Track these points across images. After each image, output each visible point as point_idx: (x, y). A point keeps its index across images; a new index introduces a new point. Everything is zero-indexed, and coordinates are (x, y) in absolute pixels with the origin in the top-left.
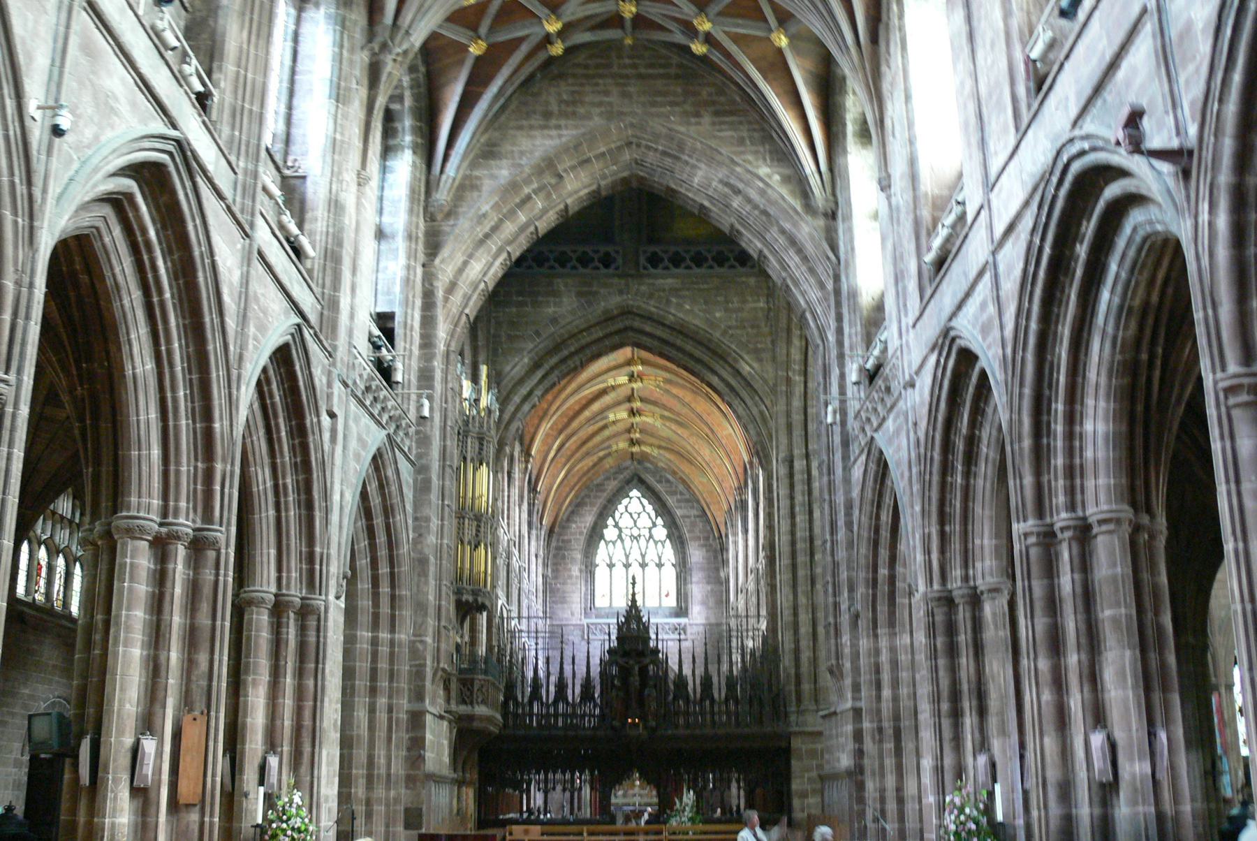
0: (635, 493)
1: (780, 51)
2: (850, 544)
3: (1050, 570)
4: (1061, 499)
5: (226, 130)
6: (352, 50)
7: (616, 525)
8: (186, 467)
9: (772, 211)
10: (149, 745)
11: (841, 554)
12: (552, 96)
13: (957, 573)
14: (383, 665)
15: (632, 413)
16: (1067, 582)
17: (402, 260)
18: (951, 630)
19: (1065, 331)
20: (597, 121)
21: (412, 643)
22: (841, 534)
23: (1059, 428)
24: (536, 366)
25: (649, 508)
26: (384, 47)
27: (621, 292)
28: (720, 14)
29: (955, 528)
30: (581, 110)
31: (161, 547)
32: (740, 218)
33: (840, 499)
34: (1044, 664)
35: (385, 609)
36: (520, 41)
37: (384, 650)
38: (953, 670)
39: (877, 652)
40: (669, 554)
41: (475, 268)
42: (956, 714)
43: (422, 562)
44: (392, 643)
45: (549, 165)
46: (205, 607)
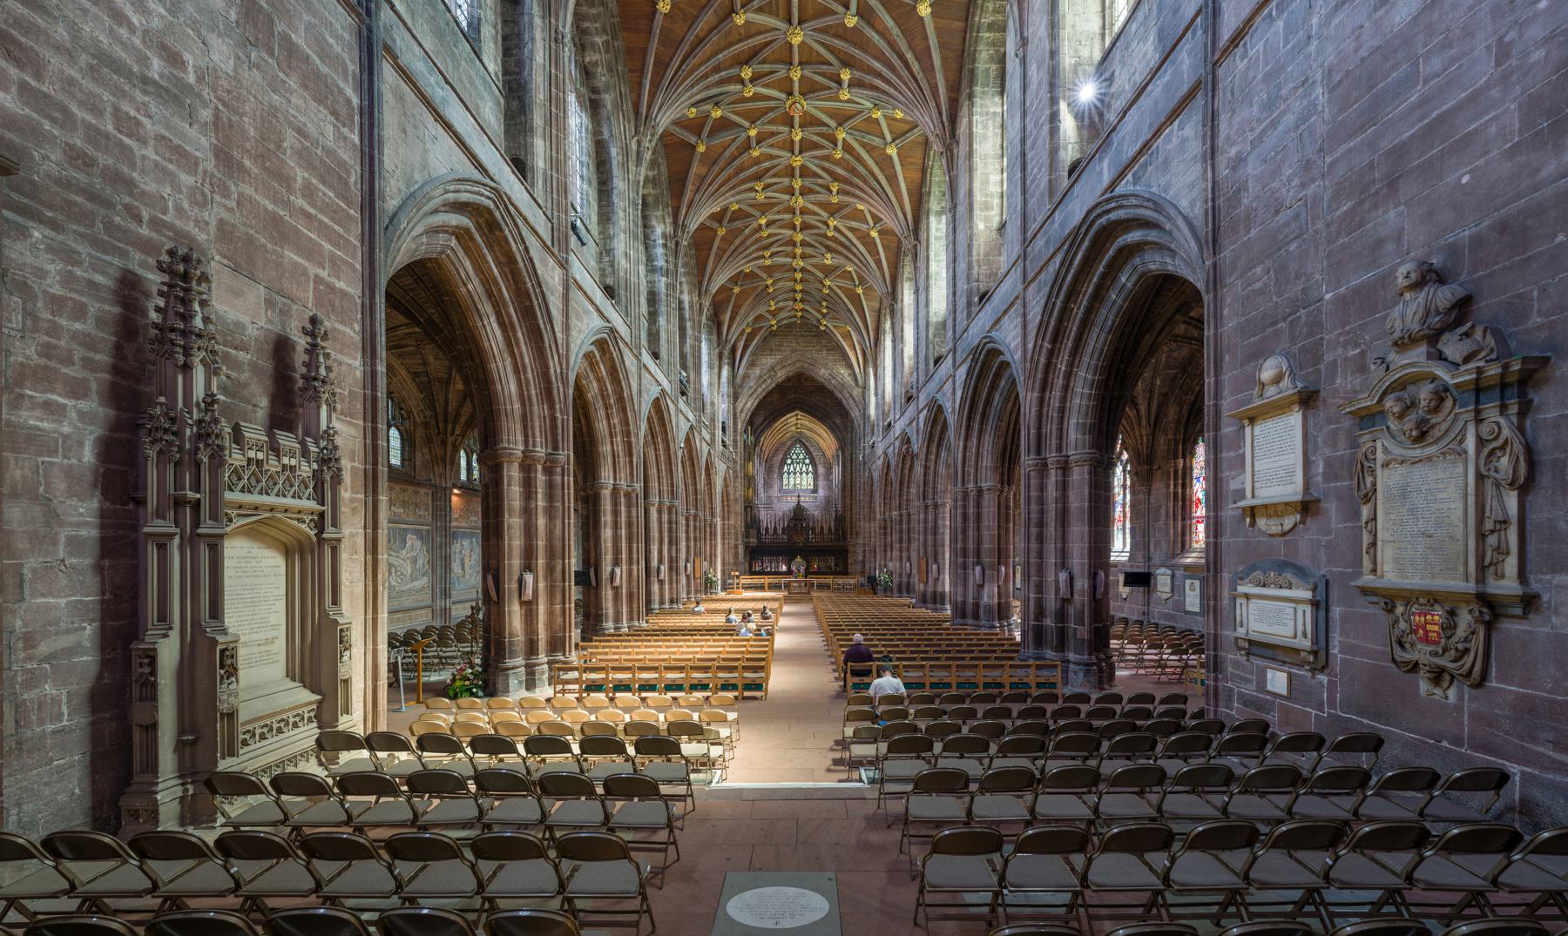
3: (901, 522)
12: (773, 343)
18: (885, 528)
45: (772, 369)
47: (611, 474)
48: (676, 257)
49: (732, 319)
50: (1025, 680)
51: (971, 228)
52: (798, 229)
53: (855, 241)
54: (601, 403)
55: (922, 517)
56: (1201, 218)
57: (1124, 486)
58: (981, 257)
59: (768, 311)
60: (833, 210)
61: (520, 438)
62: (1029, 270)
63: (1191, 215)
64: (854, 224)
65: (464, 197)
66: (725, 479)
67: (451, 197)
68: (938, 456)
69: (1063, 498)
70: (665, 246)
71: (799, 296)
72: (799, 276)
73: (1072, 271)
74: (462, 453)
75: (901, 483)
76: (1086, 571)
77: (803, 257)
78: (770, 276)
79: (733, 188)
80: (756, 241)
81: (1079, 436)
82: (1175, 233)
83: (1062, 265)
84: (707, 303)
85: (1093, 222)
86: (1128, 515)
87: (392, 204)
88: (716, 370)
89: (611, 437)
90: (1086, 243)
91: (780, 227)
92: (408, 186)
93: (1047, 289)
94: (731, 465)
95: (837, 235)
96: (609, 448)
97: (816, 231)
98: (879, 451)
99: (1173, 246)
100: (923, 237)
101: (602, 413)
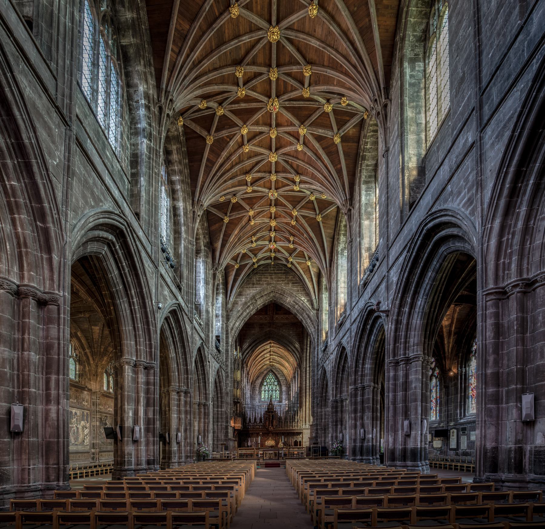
6: (209, 270)
9: (304, 309)
15: (270, 355)
26: (216, 269)
27: (269, 327)
40: (278, 388)
45: (254, 297)
78: (252, 208)
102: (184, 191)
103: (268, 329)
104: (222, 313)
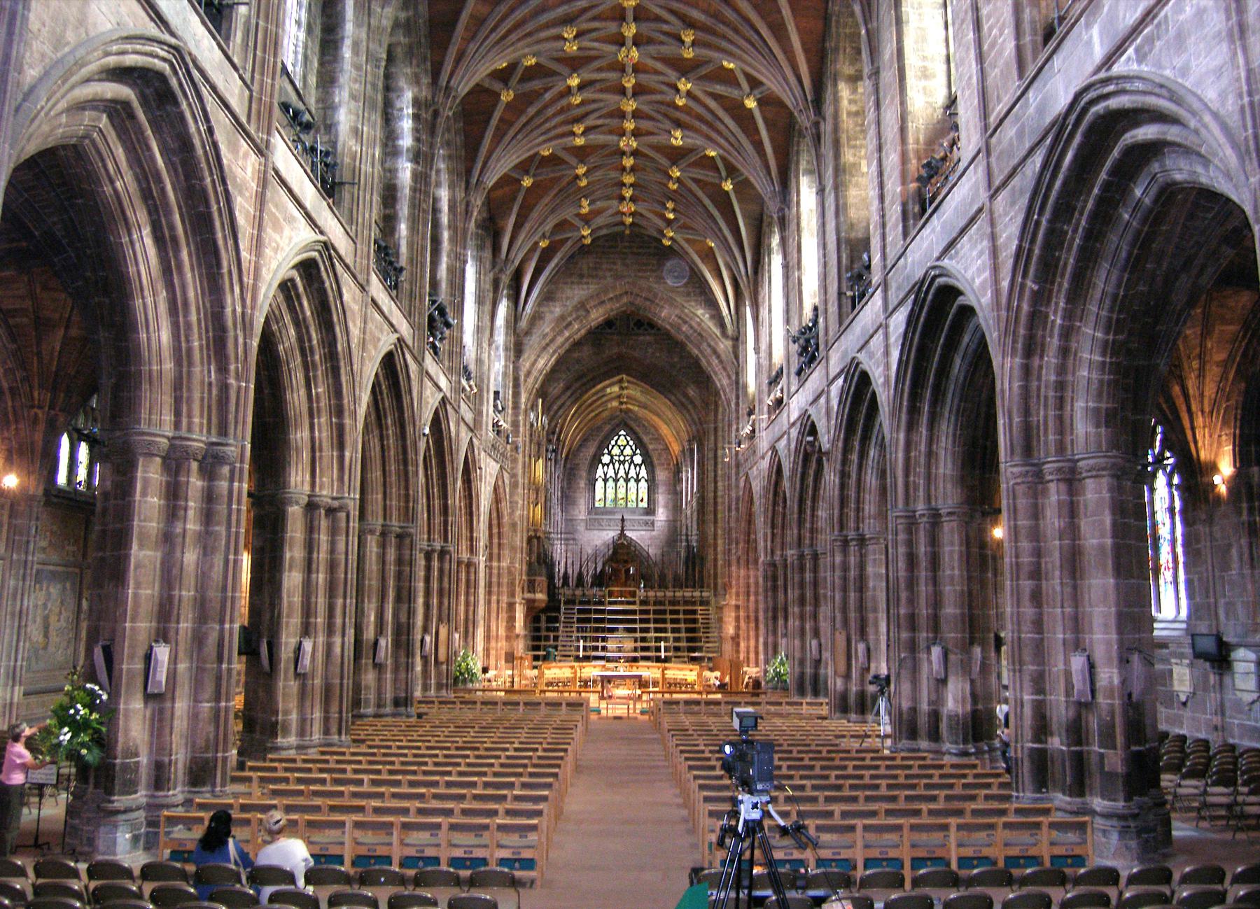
0: (622, 432)
1: (711, 248)
2: (737, 520)
3: (802, 569)
4: (807, 542)
5: (447, 363)
7: (609, 453)
8: (437, 520)
10: (428, 638)
11: (733, 525)
12: (585, 264)
13: (779, 553)
14: (495, 579)
15: (622, 388)
16: (808, 576)
17: (503, 363)
18: (775, 579)
19: (812, 472)
20: (609, 280)
21: (509, 568)
22: (734, 513)
23: (808, 512)
24: (567, 388)
25: (631, 443)
26: (501, 271)
28: (680, 227)
29: (778, 531)
30: (601, 273)
31: (428, 556)
32: (687, 337)
33: (734, 495)
34: (796, 610)
35: (495, 551)
36: (567, 239)
37: (495, 571)
38: (775, 598)
39: (749, 577)
40: (643, 473)
41: (541, 362)
42: (775, 618)
43: (514, 525)
44: (499, 568)
45: (582, 306)
46: (446, 579)
47: (308, 477)
48: (433, 133)
49: (518, 226)
50: (1032, 852)
51: (903, 103)
52: (629, 92)
53: (721, 113)
54: (299, 360)
55: (838, 559)
56: (1237, 117)
57: (1171, 510)
58: (922, 147)
59: (578, 215)
60: (685, 68)
61: (168, 418)
62: (995, 171)
63: (1222, 112)
64: (719, 89)
65: (130, 60)
66: (496, 489)
67: (112, 61)
68: (863, 455)
69: (1072, 530)
70: (416, 117)
71: (628, 193)
72: (628, 162)
73: (1061, 177)
74: (65, 441)
75: (801, 501)
76: (1115, 654)
77: (636, 134)
78: (582, 161)
79: (529, 34)
80: (562, 111)
81: (1091, 429)
82: (1203, 131)
83: (1045, 166)
84: (478, 201)
85: (1085, 110)
86: (1181, 559)
87: (32, 73)
88: (488, 307)
89: (311, 416)
90: (1078, 139)
91: (601, 91)
92: (56, 49)
93: (1024, 201)
94: (508, 464)
95: (692, 104)
96: (306, 434)
97: (658, 97)
98: (763, 443)
99: (1203, 151)
100: (828, 110)
101: (298, 376)
102: (451, 172)
103: (615, 350)
104: (506, 342)
